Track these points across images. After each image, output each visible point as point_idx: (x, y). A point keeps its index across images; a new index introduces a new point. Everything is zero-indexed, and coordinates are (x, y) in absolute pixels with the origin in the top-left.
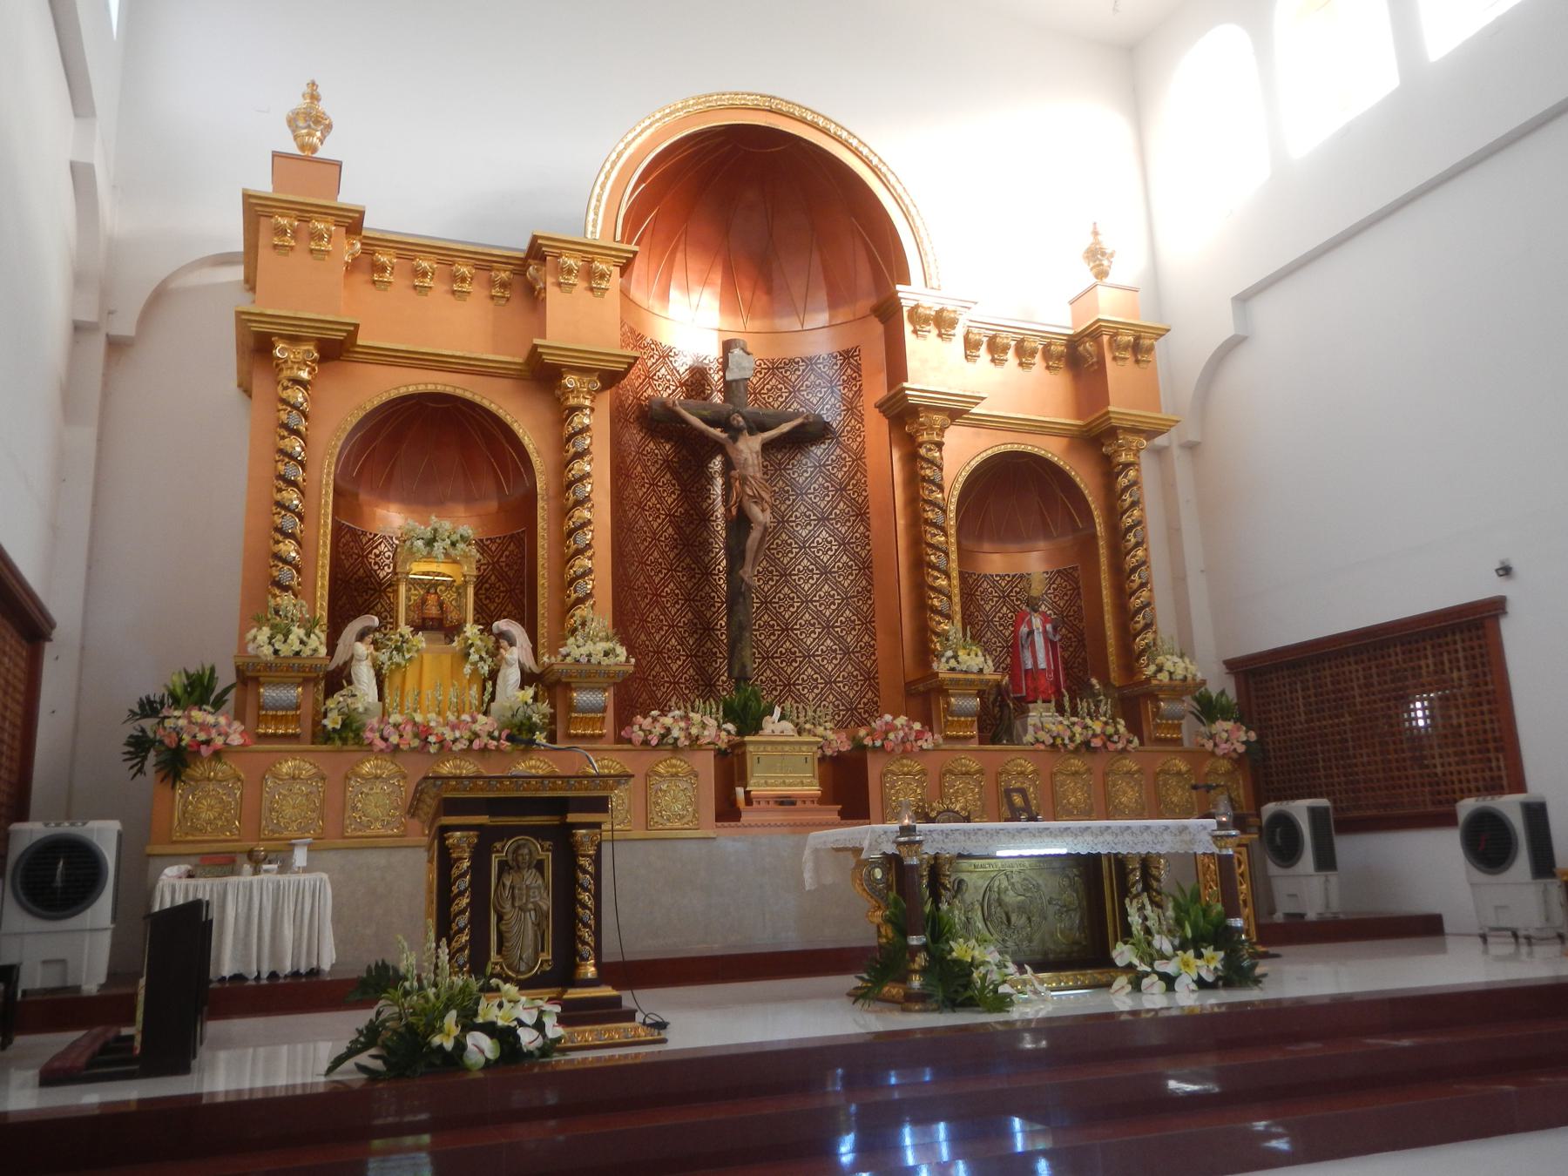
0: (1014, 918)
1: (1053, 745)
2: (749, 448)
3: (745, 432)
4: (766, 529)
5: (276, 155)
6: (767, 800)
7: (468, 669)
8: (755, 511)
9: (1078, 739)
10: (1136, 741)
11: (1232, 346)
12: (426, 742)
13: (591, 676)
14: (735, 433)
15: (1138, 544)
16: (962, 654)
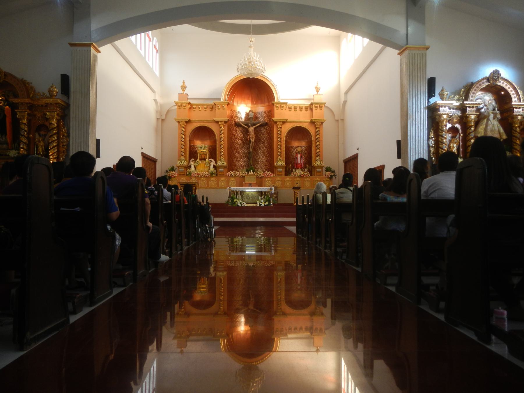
0: (250, 198)
1: (294, 176)
2: (251, 129)
3: (251, 126)
4: (253, 142)
5: (179, 94)
6: (248, 183)
7: (206, 166)
8: (251, 140)
9: (298, 175)
10: (309, 175)
11: (345, 102)
12: (199, 176)
13: (220, 167)
14: (249, 127)
15: (318, 142)
16: (279, 162)
